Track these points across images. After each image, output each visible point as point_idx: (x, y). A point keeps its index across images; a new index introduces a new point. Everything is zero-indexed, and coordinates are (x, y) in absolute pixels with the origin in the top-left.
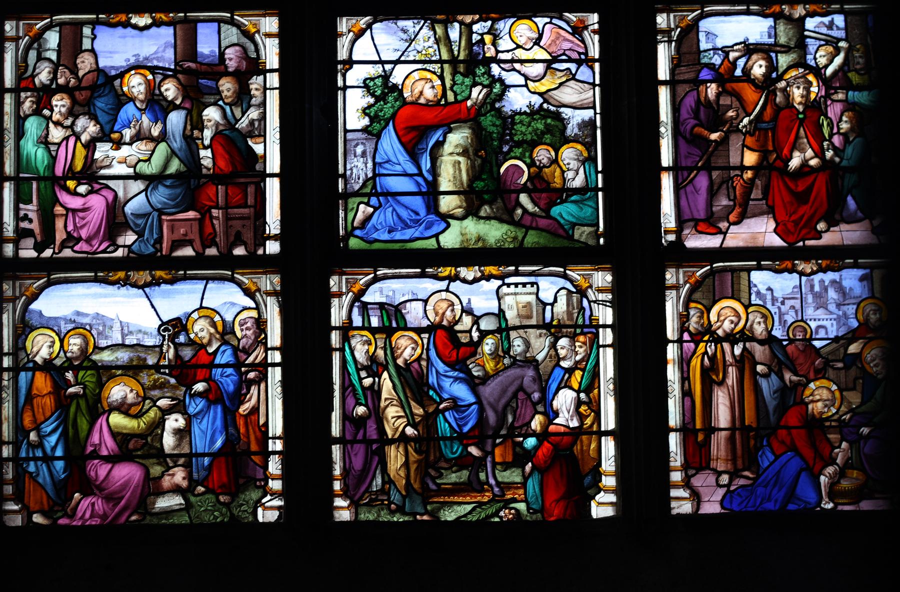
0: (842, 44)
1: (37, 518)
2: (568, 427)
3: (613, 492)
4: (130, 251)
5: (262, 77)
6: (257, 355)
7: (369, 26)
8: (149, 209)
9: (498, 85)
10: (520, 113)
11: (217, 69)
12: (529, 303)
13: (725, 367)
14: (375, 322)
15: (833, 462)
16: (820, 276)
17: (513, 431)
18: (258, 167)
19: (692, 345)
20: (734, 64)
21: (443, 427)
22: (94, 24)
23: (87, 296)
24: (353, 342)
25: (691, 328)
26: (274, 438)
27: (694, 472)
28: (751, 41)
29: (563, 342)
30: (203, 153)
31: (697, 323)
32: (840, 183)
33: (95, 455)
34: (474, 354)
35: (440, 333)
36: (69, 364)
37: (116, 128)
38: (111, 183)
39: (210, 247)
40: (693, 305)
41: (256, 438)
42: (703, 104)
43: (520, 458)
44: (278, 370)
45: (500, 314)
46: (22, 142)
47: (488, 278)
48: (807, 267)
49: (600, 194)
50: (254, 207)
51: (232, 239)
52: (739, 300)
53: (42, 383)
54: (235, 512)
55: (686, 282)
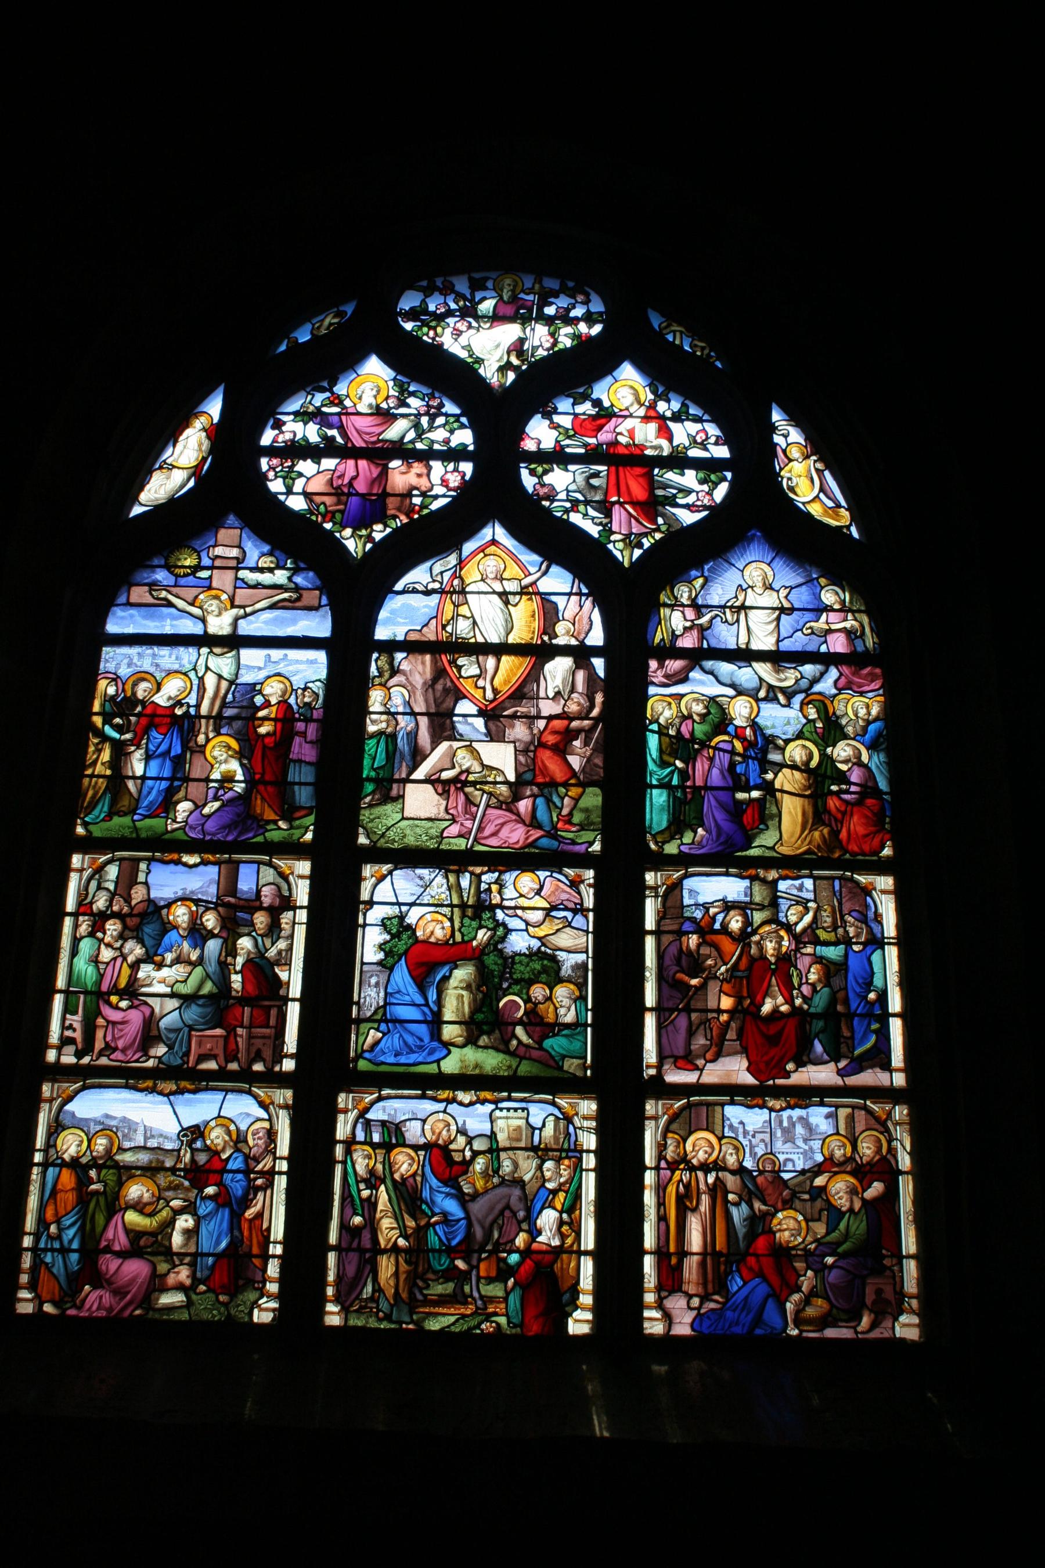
0: (811, 905)
1: (48, 1308)
2: (549, 1245)
3: (589, 1310)
4: (160, 1062)
5: (291, 913)
7: (390, 873)
8: (181, 1025)
9: (501, 929)
10: (520, 954)
11: (253, 904)
12: (519, 1127)
13: (699, 1194)
14: (376, 1138)
15: (798, 1289)
16: (789, 1112)
17: (497, 1247)
18: (282, 992)
19: (668, 1172)
20: (713, 919)
21: (433, 1240)
22: (150, 860)
23: (116, 1100)
24: (355, 1156)
25: (668, 1157)
26: (275, 1242)
27: (666, 1294)
28: (729, 899)
29: (549, 1164)
30: (234, 977)
31: (674, 1152)
32: (808, 1027)
33: (108, 1249)
34: (466, 1172)
35: (435, 1150)
36: (94, 1163)
37: (159, 952)
38: (150, 1000)
39: (232, 1061)
40: (670, 1135)
41: (259, 1243)
42: (684, 954)
43: (504, 1273)
44: (284, 1178)
45: (492, 1136)
46: (75, 960)
47: (483, 1102)
48: (777, 1104)
49: (589, 1029)
50: (275, 1027)
51: (253, 1055)
52: (713, 1132)
53: (67, 1179)
54: (233, 1312)
55: (664, 1114)
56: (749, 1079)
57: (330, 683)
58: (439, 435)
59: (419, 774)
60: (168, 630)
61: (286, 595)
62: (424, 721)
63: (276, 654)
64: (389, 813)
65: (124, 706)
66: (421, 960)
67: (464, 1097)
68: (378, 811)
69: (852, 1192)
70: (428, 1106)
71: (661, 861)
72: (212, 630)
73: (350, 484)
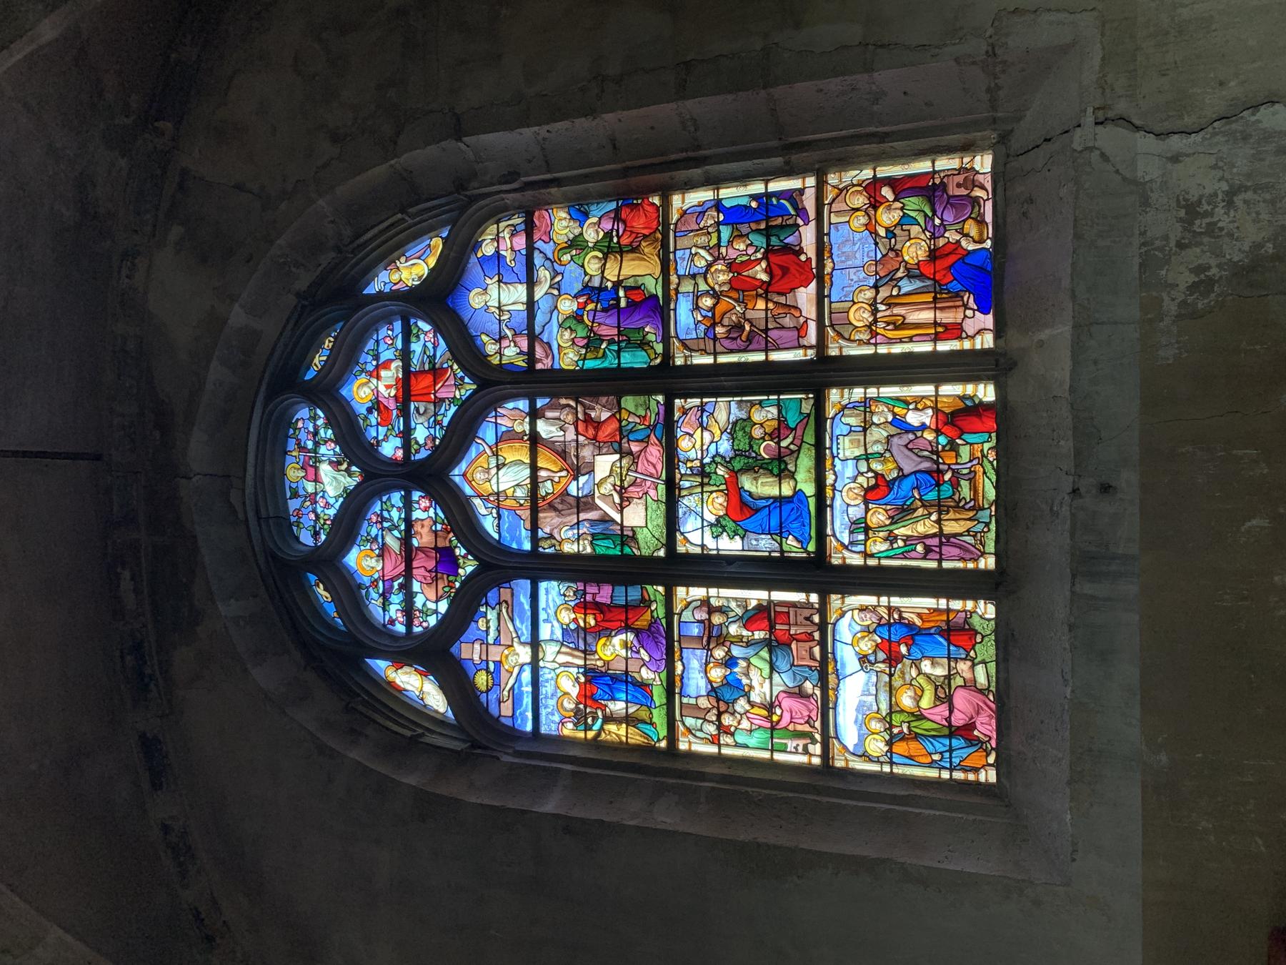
1: (991, 759)
6: (883, 612)
11: (707, 625)
14: (862, 537)
20: (705, 317)
21: (932, 496)
29: (875, 419)
30: (756, 637)
33: (948, 719)
34: (883, 476)
38: (775, 694)
43: (953, 447)
45: (857, 459)
47: (833, 466)
53: (900, 748)
56: (813, 285)
57: (561, 579)
58: (395, 514)
59: (617, 517)
60: (529, 689)
61: (504, 611)
62: (583, 516)
63: (542, 616)
64: (643, 536)
65: (580, 718)
66: (742, 510)
67: (830, 478)
68: (642, 544)
69: (889, 208)
70: (838, 503)
71: (667, 355)
72: (528, 660)
73: (430, 571)
